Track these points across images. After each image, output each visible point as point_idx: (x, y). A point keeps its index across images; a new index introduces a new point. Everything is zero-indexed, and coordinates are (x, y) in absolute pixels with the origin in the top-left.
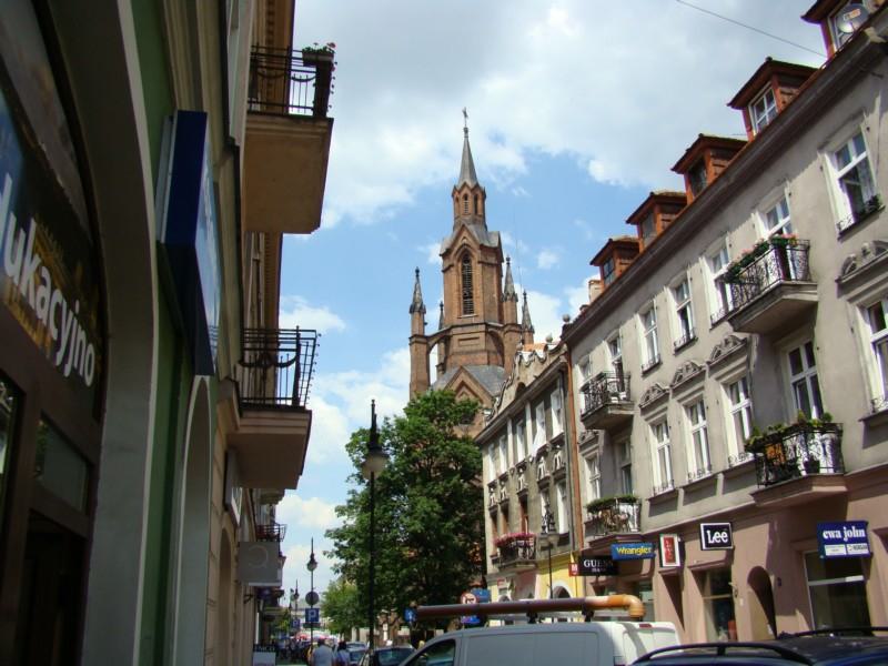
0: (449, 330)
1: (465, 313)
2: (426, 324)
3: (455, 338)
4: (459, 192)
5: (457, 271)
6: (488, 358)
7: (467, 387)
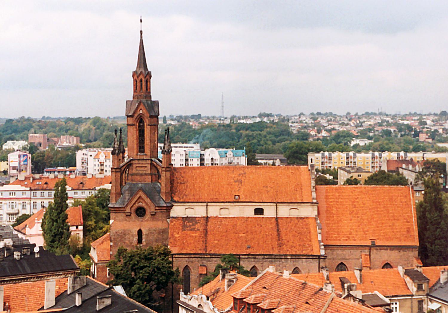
1: (140, 152)
3: (135, 166)
6: (152, 178)
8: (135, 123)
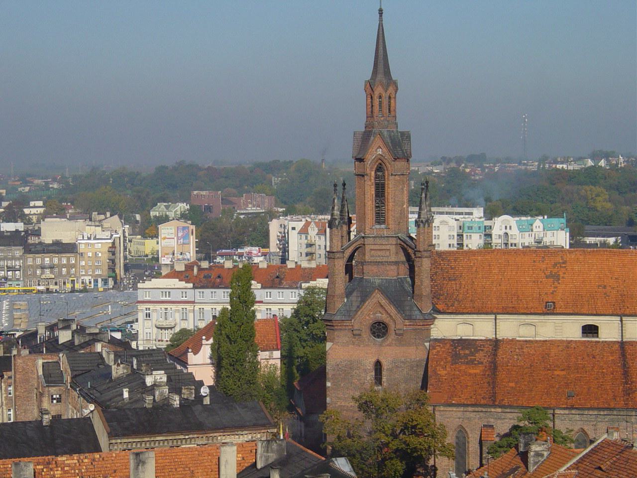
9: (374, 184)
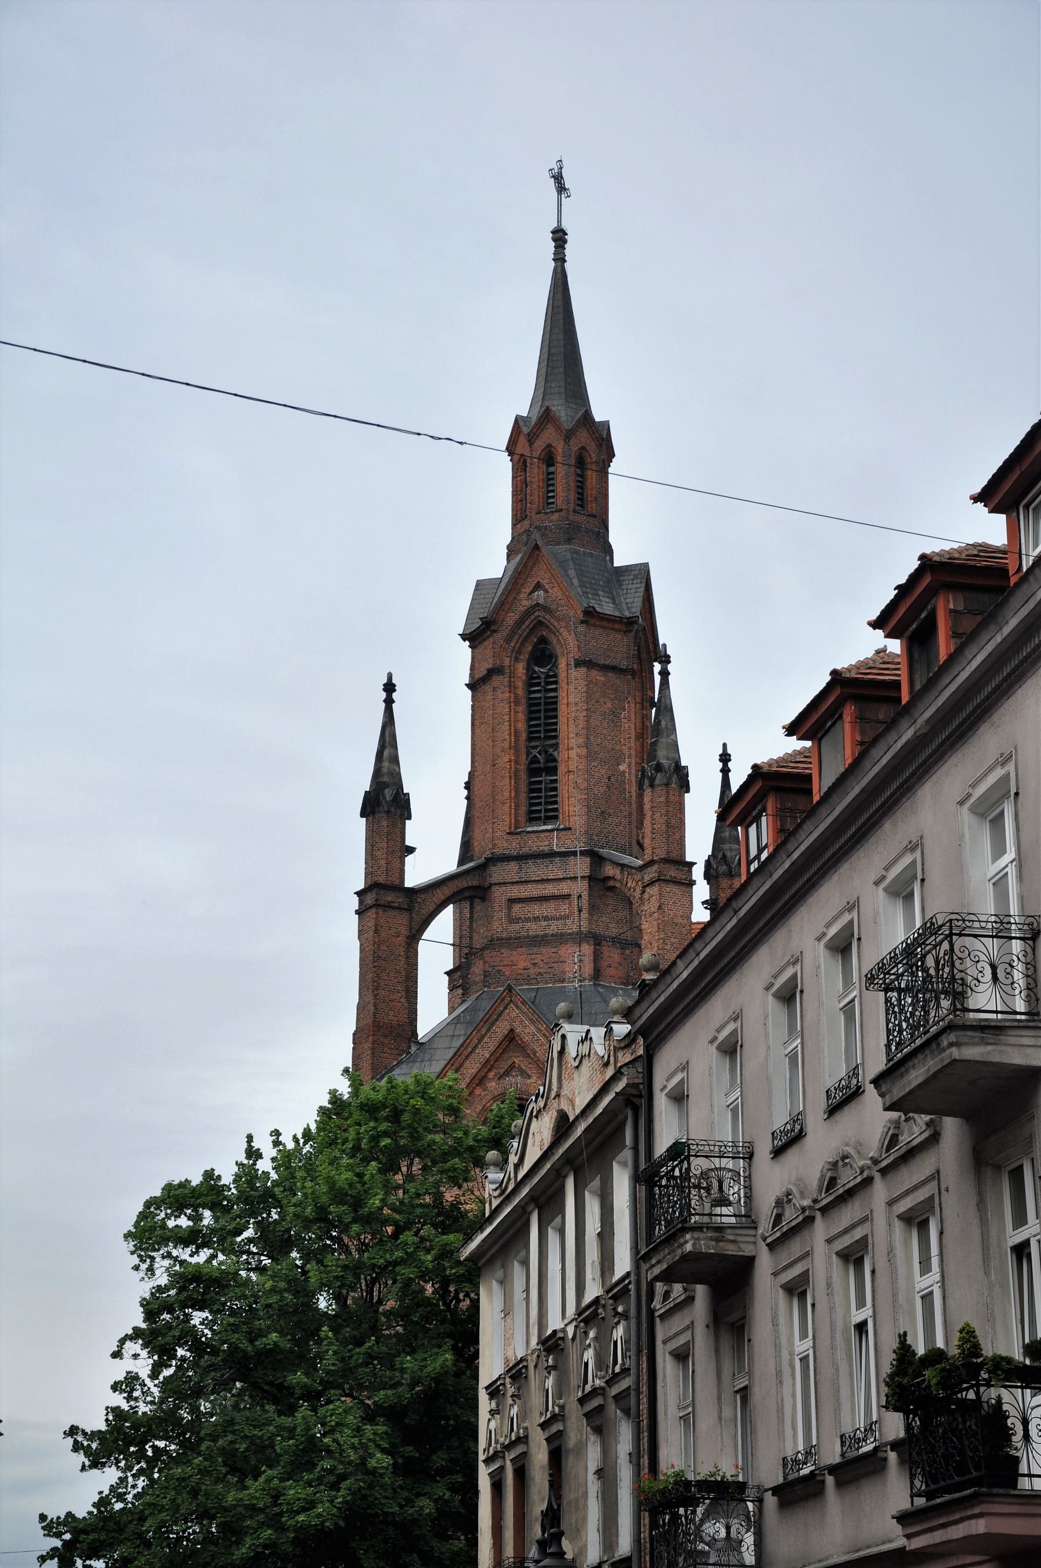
0: (482, 868)
2: (411, 850)
3: (500, 895)
4: (531, 438)
5: (512, 686)
6: (597, 957)
7: (523, 1049)
8: (507, 662)
9: (523, 701)
